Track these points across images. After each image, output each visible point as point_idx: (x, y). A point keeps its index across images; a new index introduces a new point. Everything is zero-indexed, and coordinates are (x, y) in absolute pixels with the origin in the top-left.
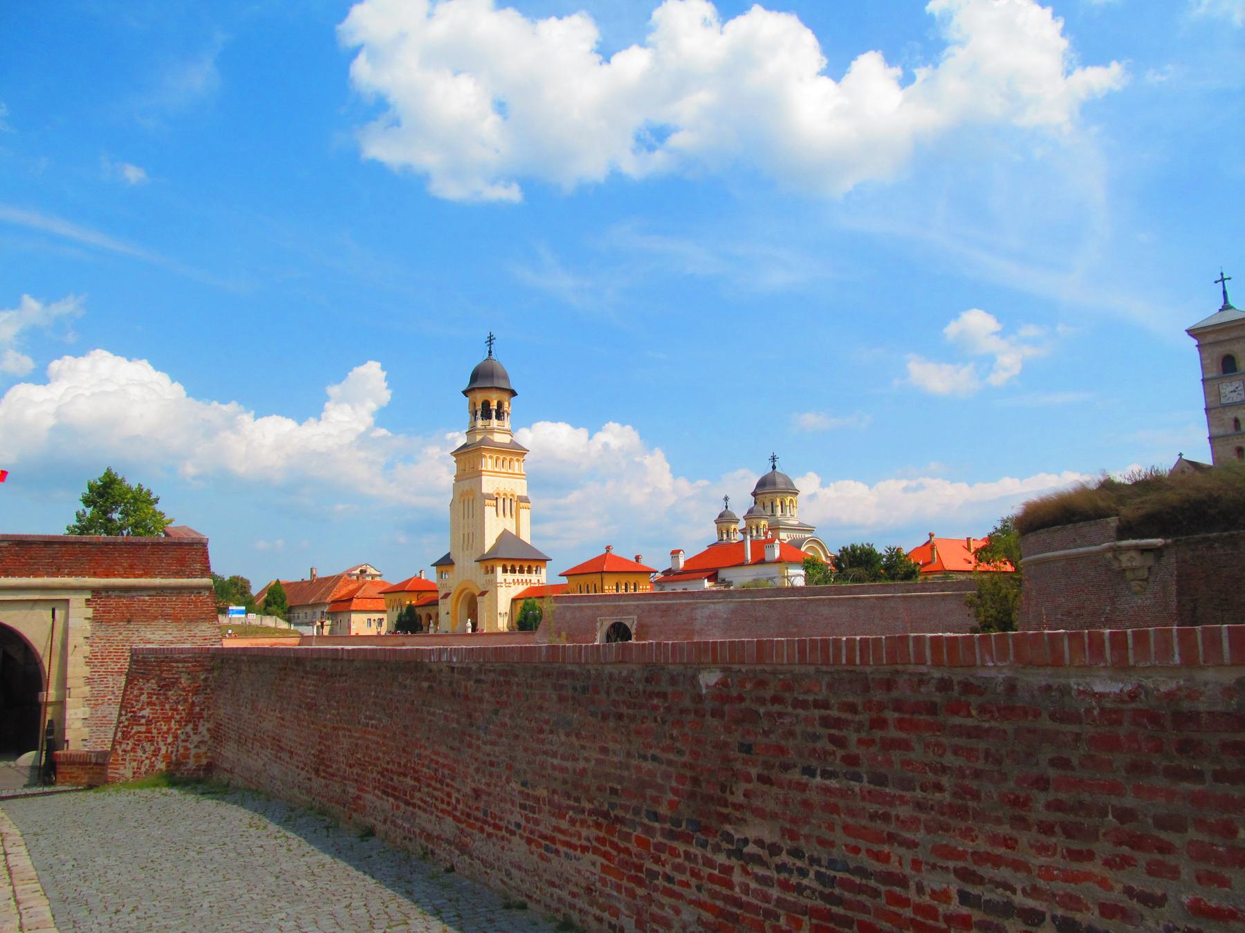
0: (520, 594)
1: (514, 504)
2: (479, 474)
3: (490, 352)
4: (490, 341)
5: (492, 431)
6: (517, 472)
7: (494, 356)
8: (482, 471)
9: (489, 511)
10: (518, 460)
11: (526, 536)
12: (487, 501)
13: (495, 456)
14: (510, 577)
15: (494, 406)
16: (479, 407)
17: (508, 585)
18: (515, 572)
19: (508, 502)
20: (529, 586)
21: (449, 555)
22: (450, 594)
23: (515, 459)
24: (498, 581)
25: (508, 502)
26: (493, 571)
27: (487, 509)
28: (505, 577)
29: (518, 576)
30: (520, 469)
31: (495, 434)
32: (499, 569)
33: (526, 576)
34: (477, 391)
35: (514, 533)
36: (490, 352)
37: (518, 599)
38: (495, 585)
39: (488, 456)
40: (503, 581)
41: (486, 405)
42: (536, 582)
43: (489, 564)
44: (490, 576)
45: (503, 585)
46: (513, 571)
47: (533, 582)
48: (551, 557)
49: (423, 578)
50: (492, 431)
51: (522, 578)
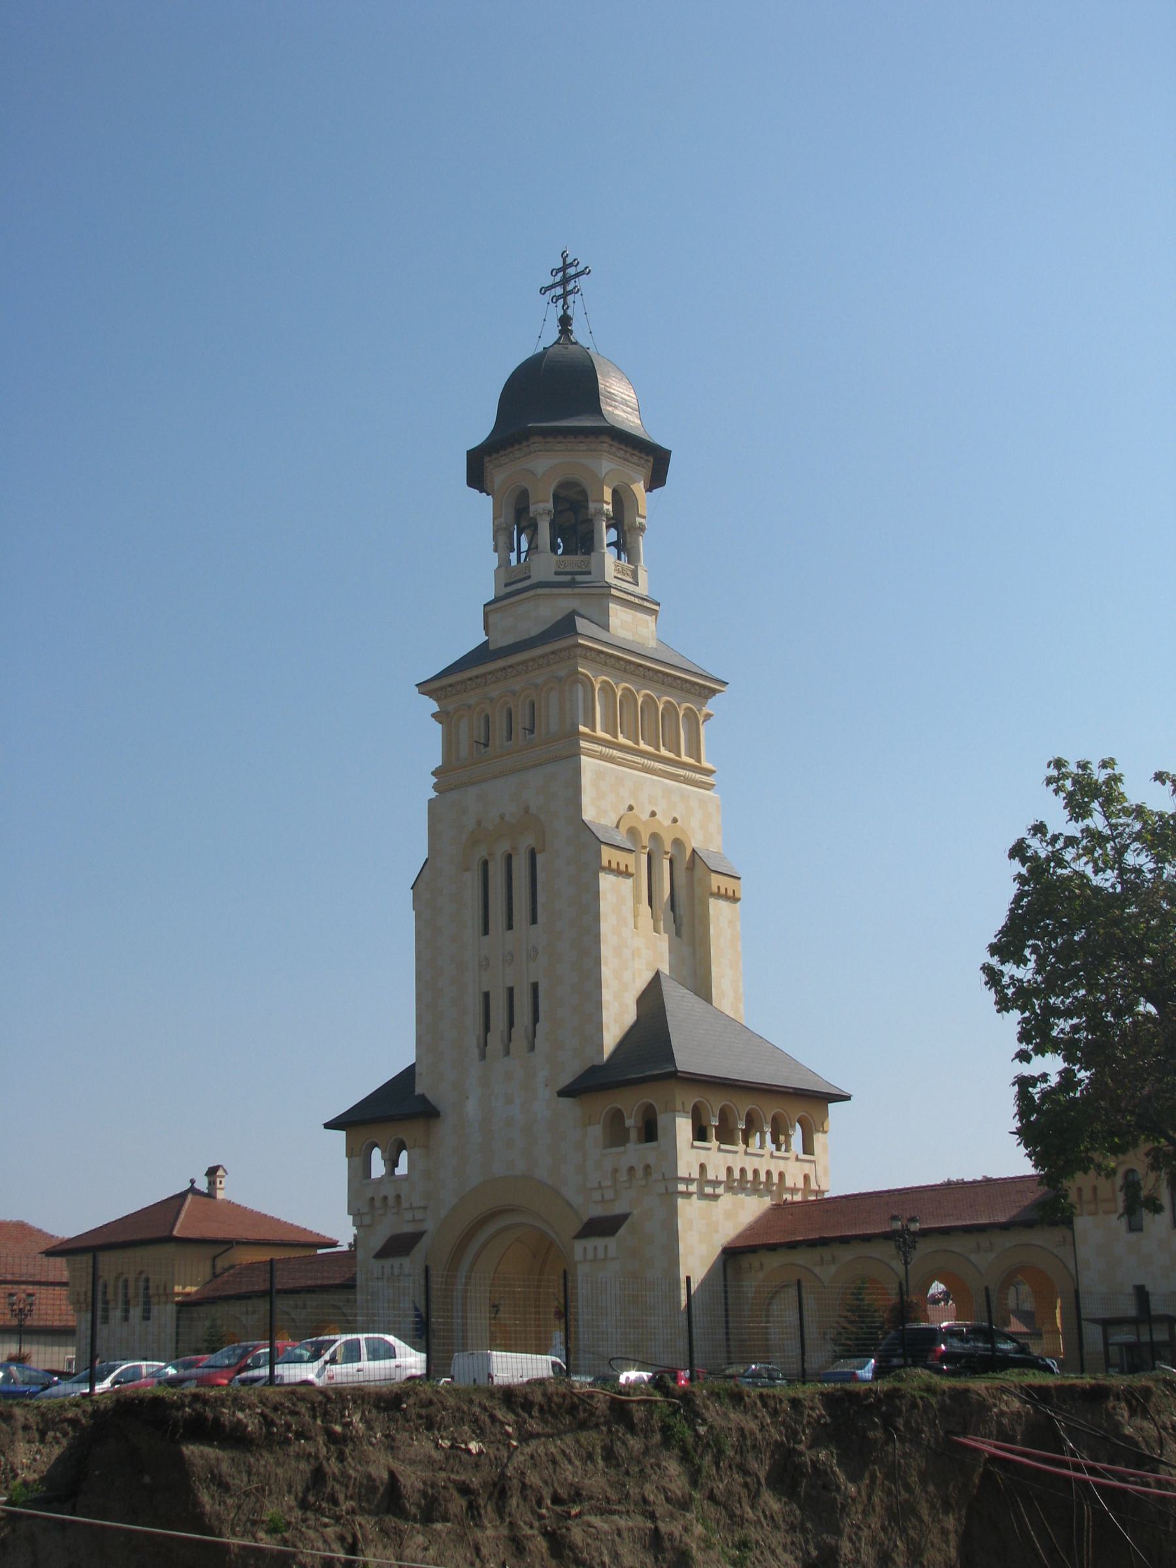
0: (752, 1229)
3: (565, 322)
4: (565, 281)
6: (685, 759)
16: (542, 506)
18: (733, 1142)
21: (408, 1075)
22: (416, 1237)
24: (682, 1172)
26: (649, 1131)
27: (606, 882)
34: (536, 439)
36: (565, 322)
37: (752, 1250)
43: (630, 1104)
44: (635, 1153)
45: (693, 1188)
46: (726, 1135)
47: (789, 1183)
48: (846, 1089)
49: (220, 1195)
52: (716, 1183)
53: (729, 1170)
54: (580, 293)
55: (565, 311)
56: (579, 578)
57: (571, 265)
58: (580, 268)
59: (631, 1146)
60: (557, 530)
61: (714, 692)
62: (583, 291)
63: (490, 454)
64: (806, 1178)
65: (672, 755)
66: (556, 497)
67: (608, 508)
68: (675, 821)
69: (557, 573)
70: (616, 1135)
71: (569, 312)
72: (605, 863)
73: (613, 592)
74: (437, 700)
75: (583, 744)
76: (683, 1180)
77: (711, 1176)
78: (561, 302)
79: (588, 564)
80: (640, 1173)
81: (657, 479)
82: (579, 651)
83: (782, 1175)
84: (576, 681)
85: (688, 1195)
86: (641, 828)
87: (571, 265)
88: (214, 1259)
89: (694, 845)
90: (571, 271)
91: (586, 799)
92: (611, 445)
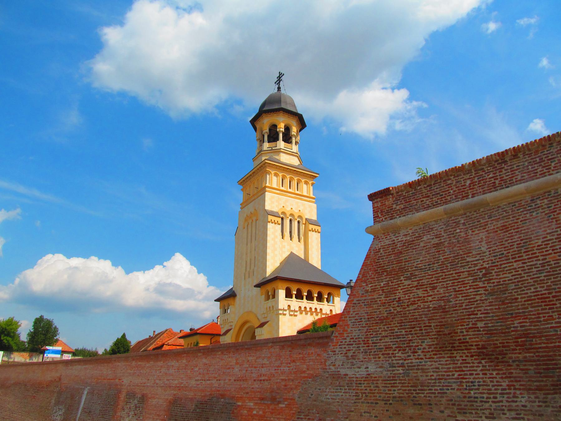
1: (302, 227)
2: (262, 191)
5: (279, 151)
6: (305, 193)
7: (283, 91)
8: (266, 187)
9: (273, 230)
10: (306, 183)
11: (315, 260)
12: (270, 218)
13: (281, 174)
14: (295, 303)
17: (293, 314)
18: (302, 298)
19: (295, 224)
20: (319, 316)
23: (303, 180)
24: (281, 307)
25: (295, 224)
26: (274, 295)
27: (270, 226)
28: (289, 303)
29: (305, 303)
30: (308, 191)
31: (282, 154)
32: (282, 293)
33: (315, 304)
35: (303, 257)
36: (279, 88)
38: (275, 312)
39: (273, 172)
40: (286, 308)
41: (273, 128)
42: (328, 312)
44: (271, 302)
45: (287, 312)
46: (299, 296)
47: (324, 312)
50: (279, 151)
51: (311, 305)
52: (295, 311)
53: (300, 307)
56: (273, 148)
59: (270, 300)
60: (269, 136)
64: (331, 311)
65: (301, 193)
66: (270, 130)
68: (300, 211)
70: (268, 298)
72: (269, 220)
73: (282, 150)
75: (267, 189)
76: (281, 310)
77: (292, 308)
79: (276, 145)
80: (271, 309)
82: (267, 164)
83: (321, 309)
84: (267, 173)
85: (285, 315)
86: (286, 212)
88: (211, 339)
89: (306, 217)
91: (266, 204)
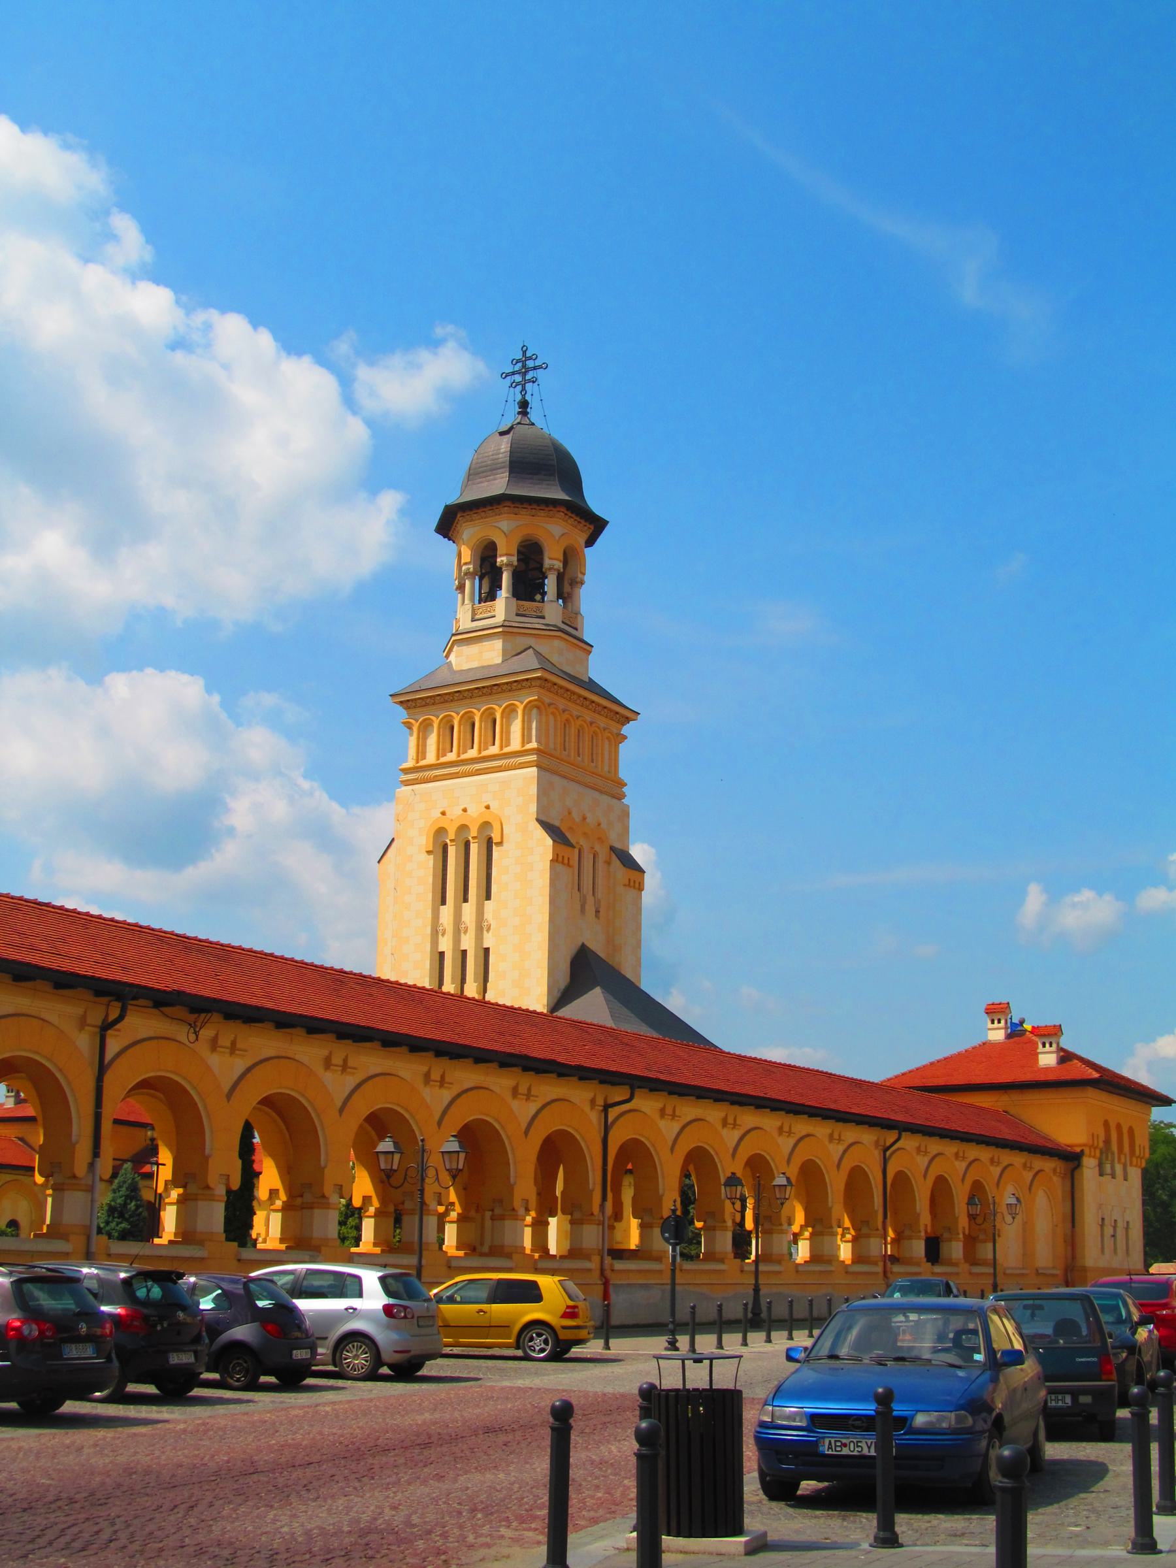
3: (524, 405)
4: (524, 371)
15: (552, 560)
36: (524, 405)
41: (530, 553)
54: (537, 383)
55: (524, 396)
57: (530, 358)
58: (538, 363)
60: (517, 577)
61: (627, 720)
62: (539, 381)
63: (464, 511)
67: (559, 565)
69: (517, 615)
71: (528, 397)
74: (407, 708)
78: (519, 388)
81: (590, 542)
87: (530, 358)
90: (530, 364)
92: (566, 514)
